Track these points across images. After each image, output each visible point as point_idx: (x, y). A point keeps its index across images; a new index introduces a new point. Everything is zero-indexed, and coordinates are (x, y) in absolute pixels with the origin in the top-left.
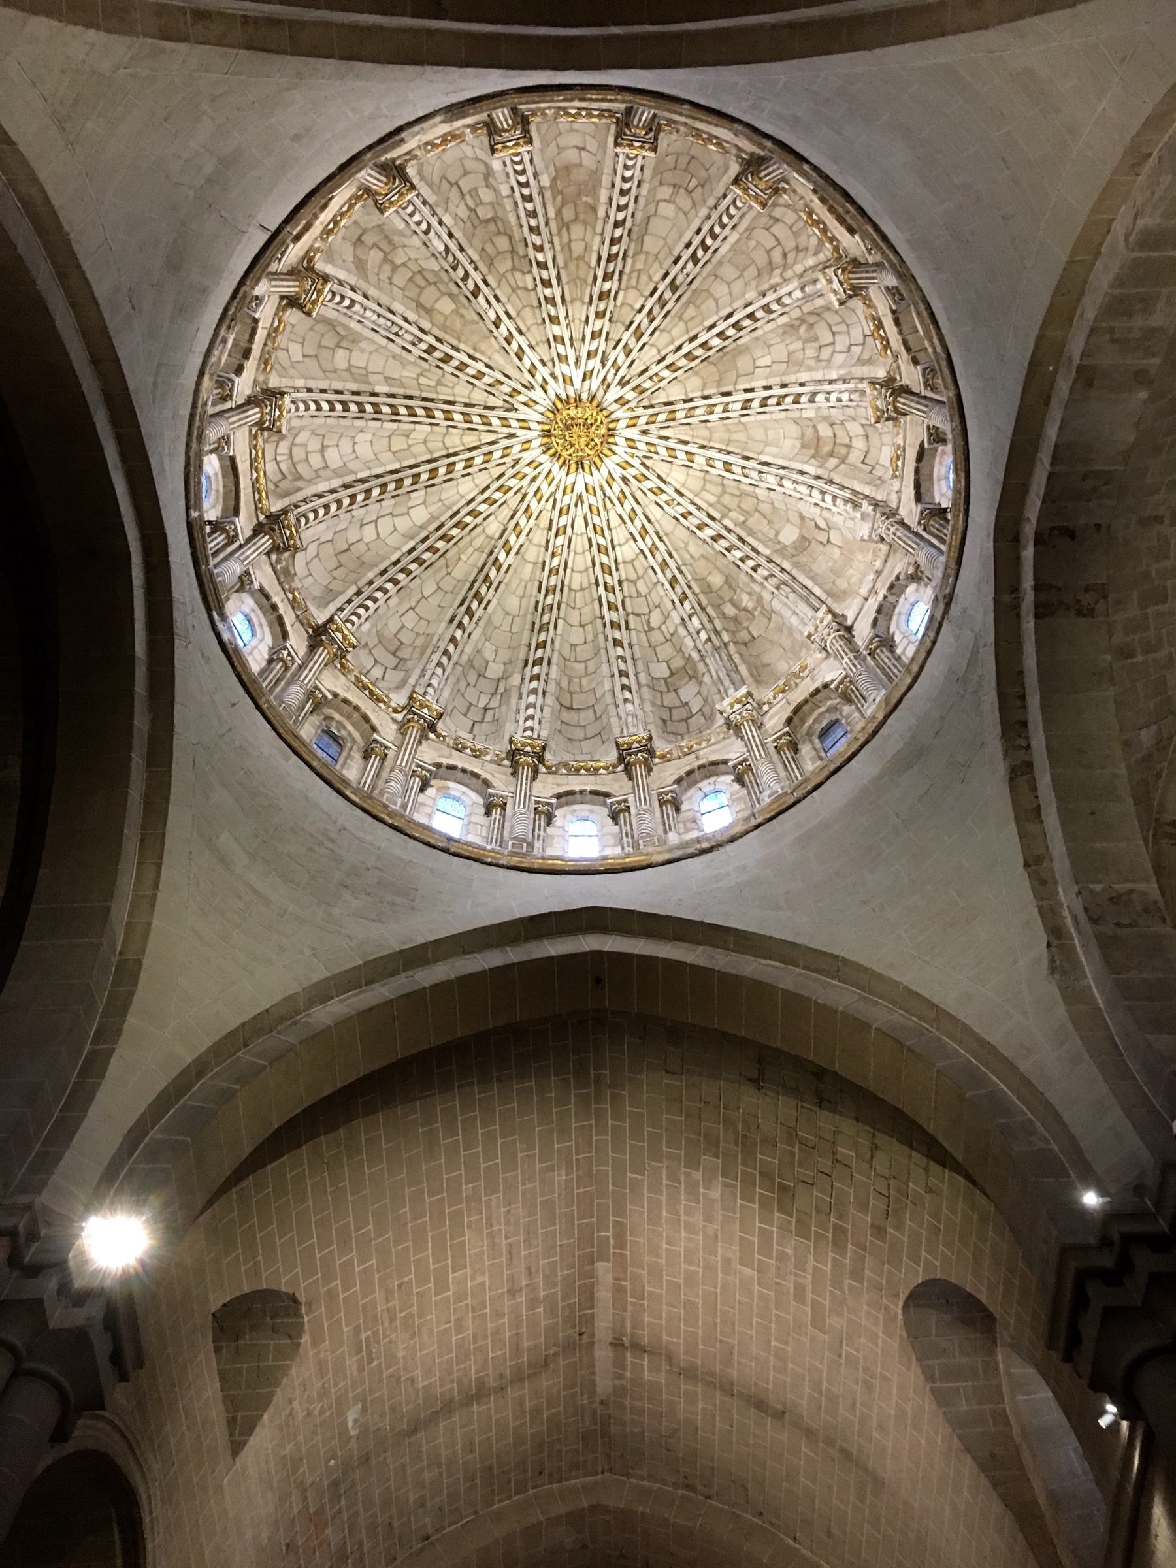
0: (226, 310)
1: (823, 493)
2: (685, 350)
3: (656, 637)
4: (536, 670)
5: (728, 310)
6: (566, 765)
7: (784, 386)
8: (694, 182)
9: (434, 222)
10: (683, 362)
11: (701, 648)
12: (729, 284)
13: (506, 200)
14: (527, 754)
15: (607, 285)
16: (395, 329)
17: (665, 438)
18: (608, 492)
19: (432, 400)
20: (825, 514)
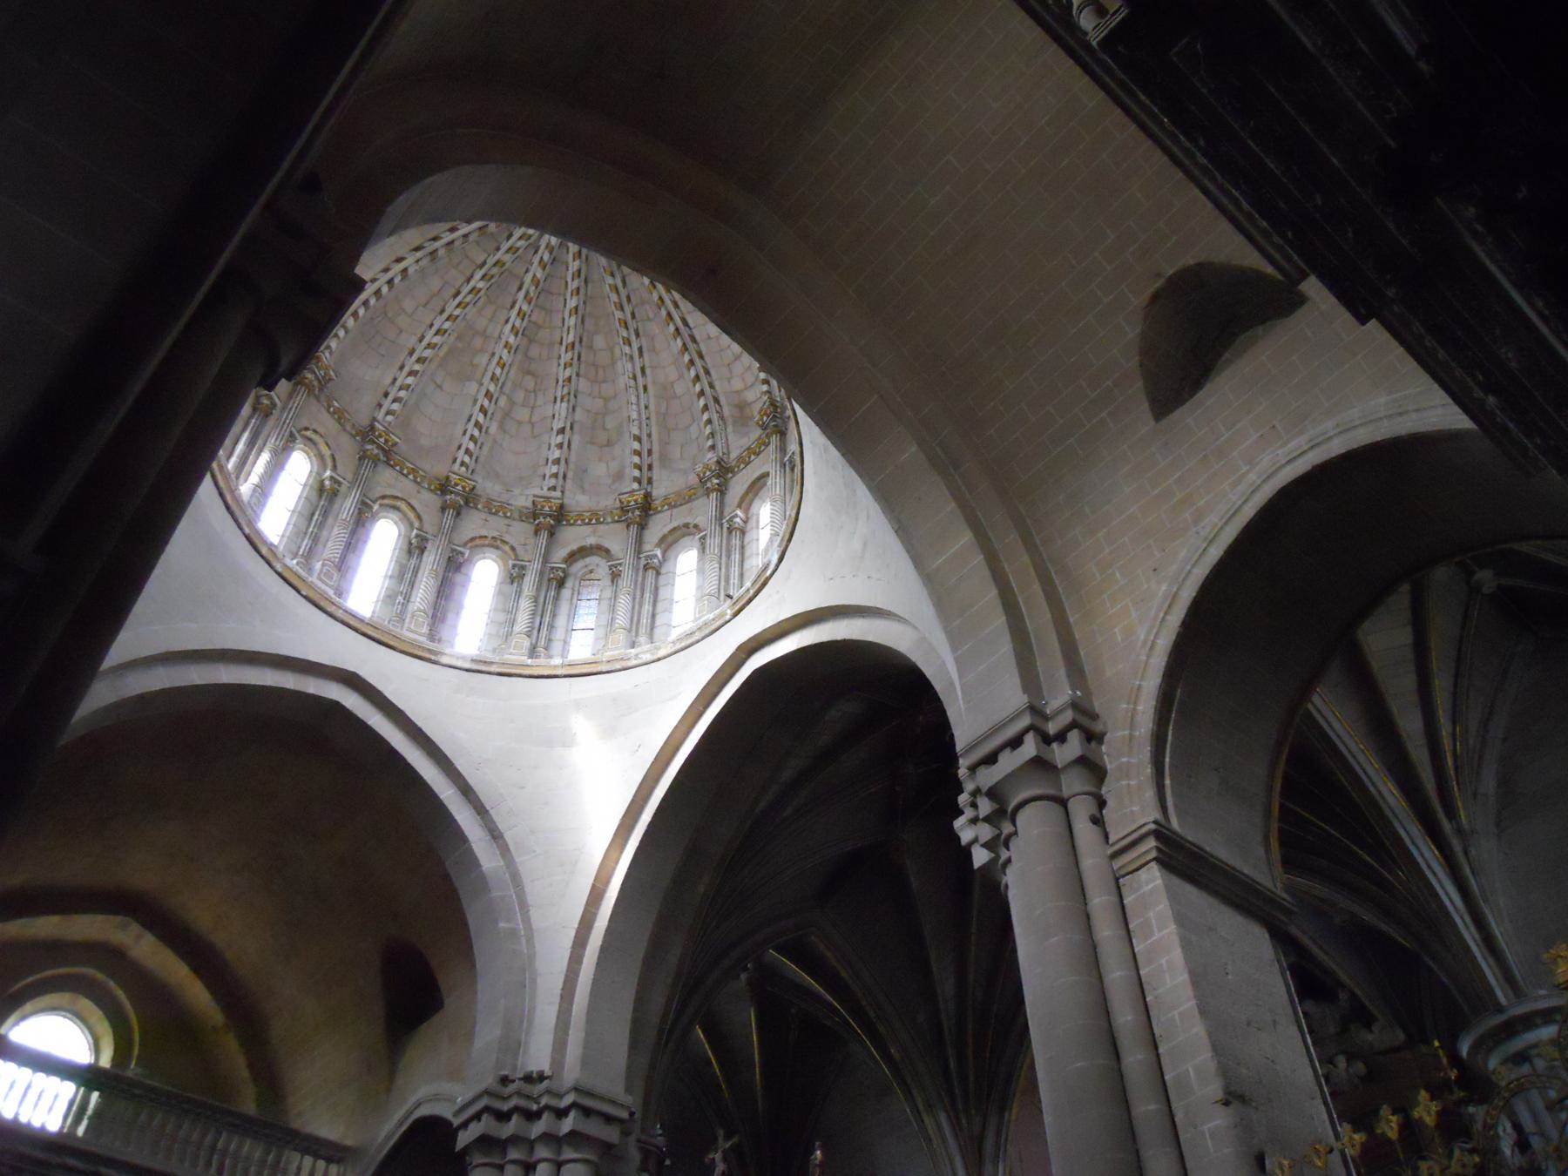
0: (620, 670)
13: (507, 392)
15: (481, 285)
16: (632, 383)
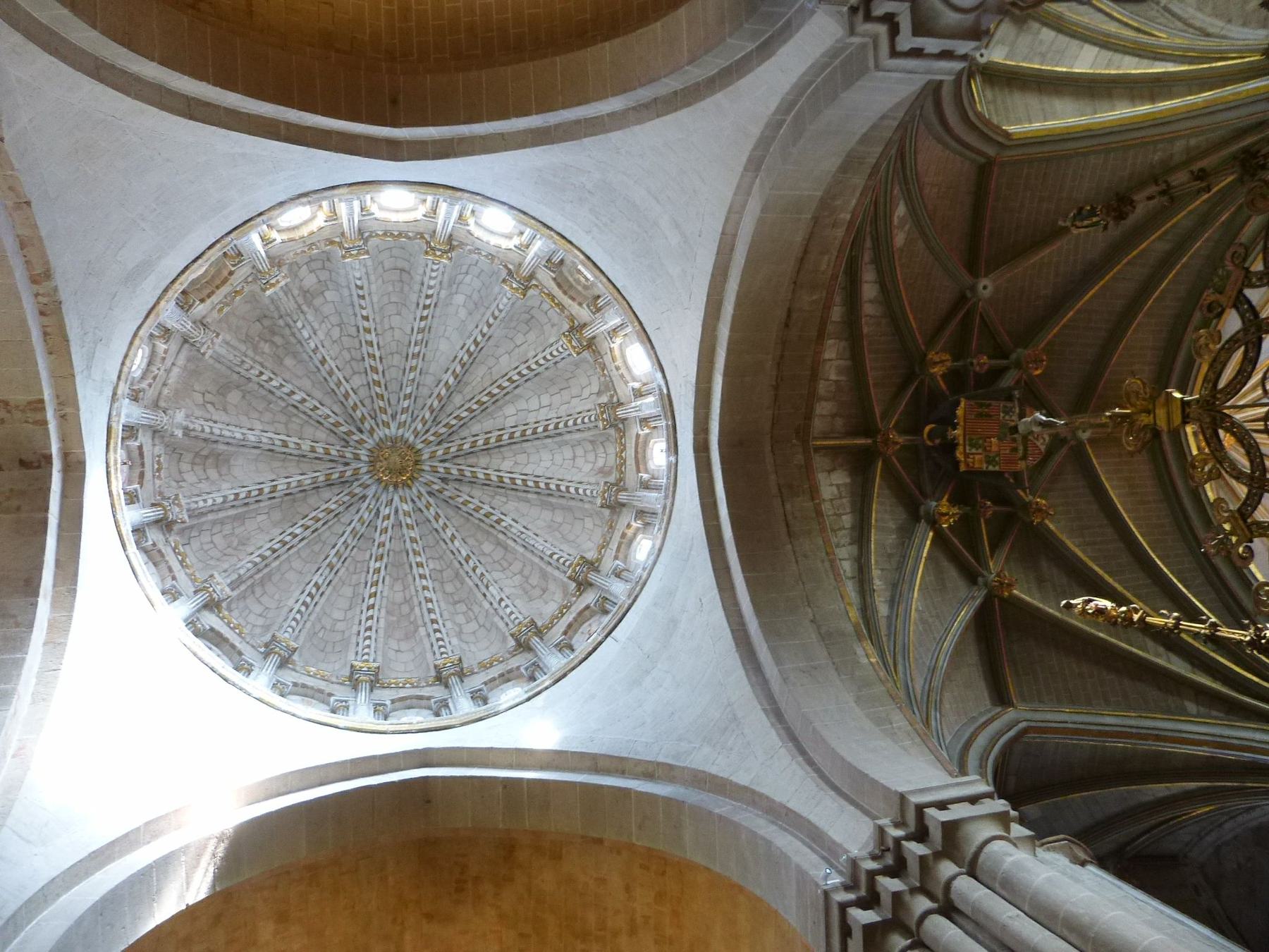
1: (212, 433)
2: (321, 522)
3: (334, 319)
4: (428, 302)
5: (291, 552)
6: (409, 238)
7: (246, 504)
8: (321, 635)
9: (495, 605)
10: (321, 516)
11: (301, 315)
12: (291, 567)
14: (439, 250)
15: (378, 565)
16: (523, 536)
17: (331, 461)
18: (373, 422)
19: (498, 487)
20: (208, 416)
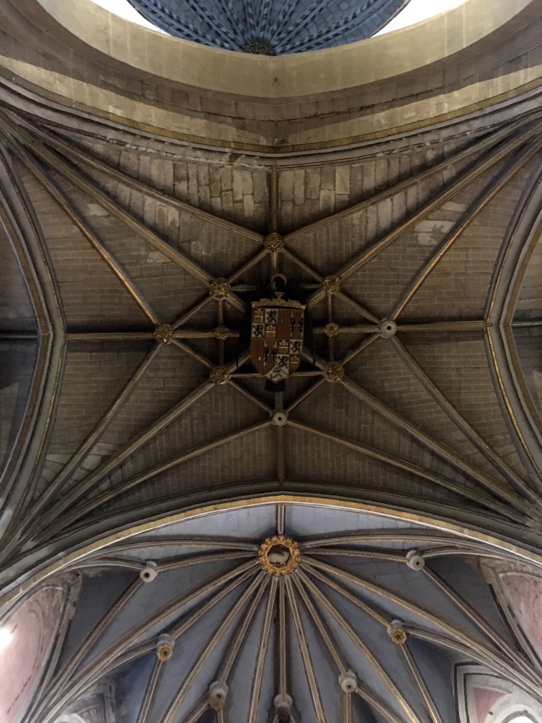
18: (284, 42)
